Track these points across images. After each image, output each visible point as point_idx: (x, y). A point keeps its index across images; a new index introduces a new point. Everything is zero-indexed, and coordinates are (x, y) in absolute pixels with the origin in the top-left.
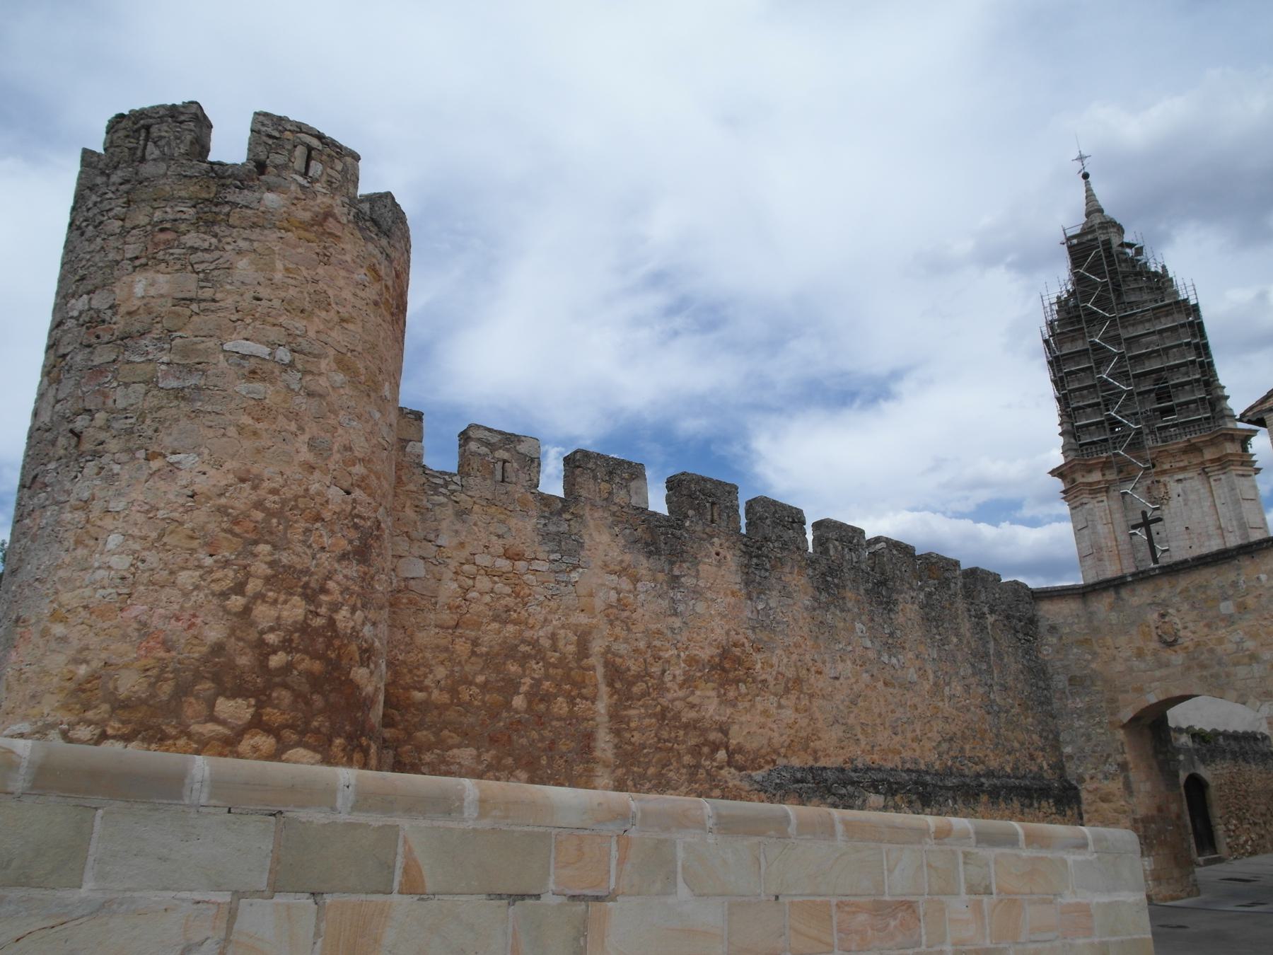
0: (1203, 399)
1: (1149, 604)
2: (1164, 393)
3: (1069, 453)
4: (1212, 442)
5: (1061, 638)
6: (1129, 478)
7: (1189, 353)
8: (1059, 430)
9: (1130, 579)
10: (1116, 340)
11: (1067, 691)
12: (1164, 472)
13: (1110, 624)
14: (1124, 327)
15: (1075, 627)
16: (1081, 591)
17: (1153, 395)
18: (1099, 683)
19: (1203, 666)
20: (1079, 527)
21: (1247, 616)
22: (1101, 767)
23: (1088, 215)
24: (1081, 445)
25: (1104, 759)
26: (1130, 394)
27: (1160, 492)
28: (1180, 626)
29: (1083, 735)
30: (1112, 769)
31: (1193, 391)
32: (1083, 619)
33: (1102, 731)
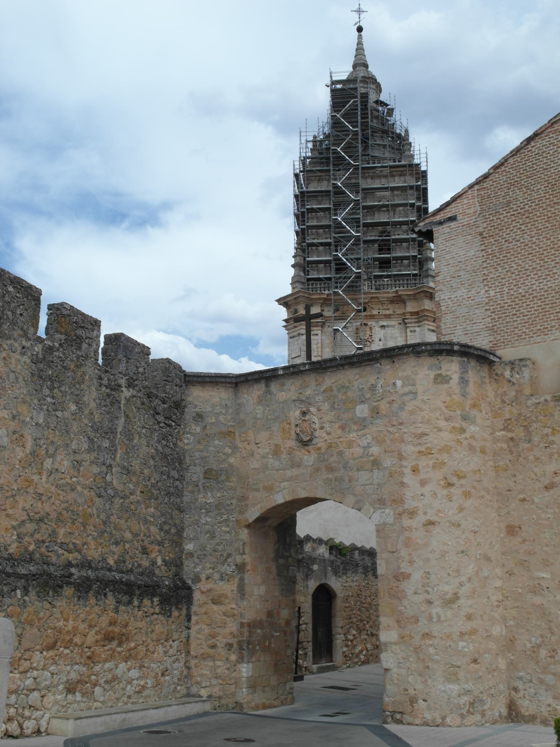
0: (415, 257)
1: (295, 400)
2: (385, 245)
3: (297, 285)
4: (415, 297)
5: (204, 428)
6: (342, 318)
7: (412, 213)
8: (293, 261)
9: (281, 372)
10: (355, 188)
11: (200, 484)
12: (372, 317)
13: (256, 419)
14: (364, 177)
15: (222, 418)
16: (234, 380)
17: (376, 245)
18: (234, 479)
19: (330, 469)
20: (293, 356)
21: (377, 421)
22: (219, 566)
23: (355, 66)
24: (309, 280)
25: (222, 559)
26: (358, 239)
28: (317, 426)
29: (208, 532)
30: (229, 569)
31: (408, 248)
32: (231, 411)
33: (227, 529)
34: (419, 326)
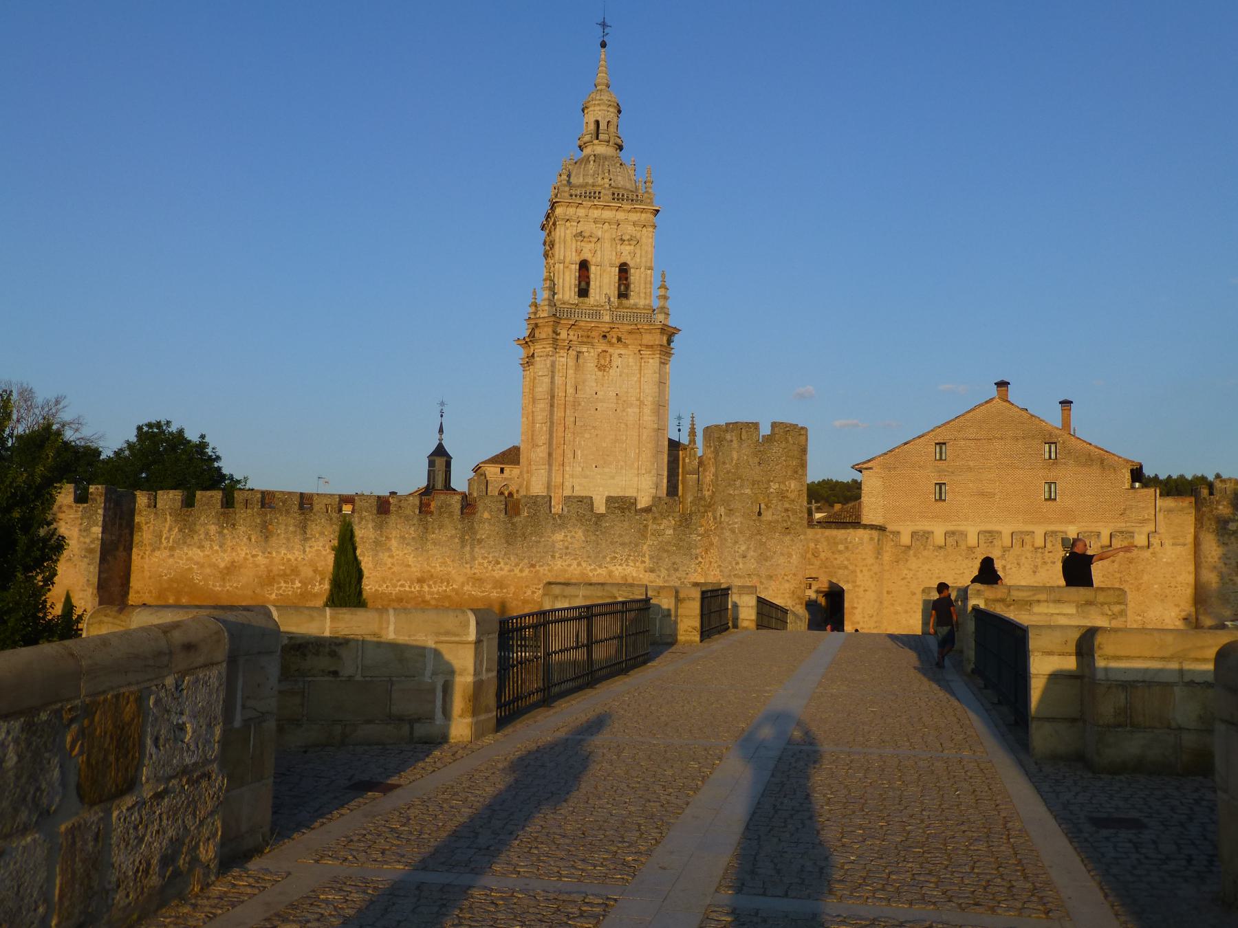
19: (826, 567)
27: (605, 361)
34: (653, 358)
